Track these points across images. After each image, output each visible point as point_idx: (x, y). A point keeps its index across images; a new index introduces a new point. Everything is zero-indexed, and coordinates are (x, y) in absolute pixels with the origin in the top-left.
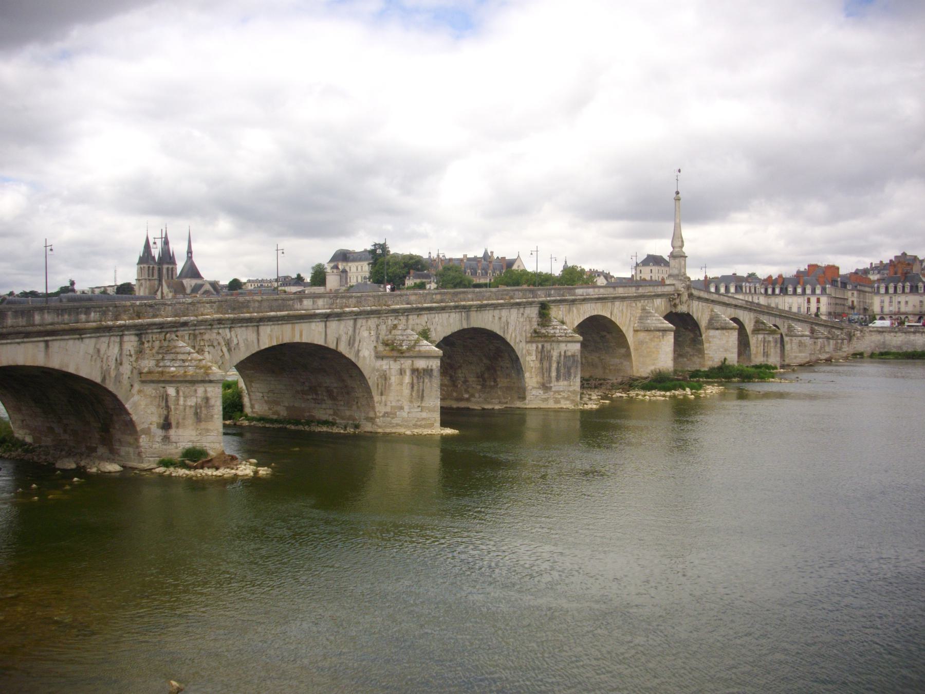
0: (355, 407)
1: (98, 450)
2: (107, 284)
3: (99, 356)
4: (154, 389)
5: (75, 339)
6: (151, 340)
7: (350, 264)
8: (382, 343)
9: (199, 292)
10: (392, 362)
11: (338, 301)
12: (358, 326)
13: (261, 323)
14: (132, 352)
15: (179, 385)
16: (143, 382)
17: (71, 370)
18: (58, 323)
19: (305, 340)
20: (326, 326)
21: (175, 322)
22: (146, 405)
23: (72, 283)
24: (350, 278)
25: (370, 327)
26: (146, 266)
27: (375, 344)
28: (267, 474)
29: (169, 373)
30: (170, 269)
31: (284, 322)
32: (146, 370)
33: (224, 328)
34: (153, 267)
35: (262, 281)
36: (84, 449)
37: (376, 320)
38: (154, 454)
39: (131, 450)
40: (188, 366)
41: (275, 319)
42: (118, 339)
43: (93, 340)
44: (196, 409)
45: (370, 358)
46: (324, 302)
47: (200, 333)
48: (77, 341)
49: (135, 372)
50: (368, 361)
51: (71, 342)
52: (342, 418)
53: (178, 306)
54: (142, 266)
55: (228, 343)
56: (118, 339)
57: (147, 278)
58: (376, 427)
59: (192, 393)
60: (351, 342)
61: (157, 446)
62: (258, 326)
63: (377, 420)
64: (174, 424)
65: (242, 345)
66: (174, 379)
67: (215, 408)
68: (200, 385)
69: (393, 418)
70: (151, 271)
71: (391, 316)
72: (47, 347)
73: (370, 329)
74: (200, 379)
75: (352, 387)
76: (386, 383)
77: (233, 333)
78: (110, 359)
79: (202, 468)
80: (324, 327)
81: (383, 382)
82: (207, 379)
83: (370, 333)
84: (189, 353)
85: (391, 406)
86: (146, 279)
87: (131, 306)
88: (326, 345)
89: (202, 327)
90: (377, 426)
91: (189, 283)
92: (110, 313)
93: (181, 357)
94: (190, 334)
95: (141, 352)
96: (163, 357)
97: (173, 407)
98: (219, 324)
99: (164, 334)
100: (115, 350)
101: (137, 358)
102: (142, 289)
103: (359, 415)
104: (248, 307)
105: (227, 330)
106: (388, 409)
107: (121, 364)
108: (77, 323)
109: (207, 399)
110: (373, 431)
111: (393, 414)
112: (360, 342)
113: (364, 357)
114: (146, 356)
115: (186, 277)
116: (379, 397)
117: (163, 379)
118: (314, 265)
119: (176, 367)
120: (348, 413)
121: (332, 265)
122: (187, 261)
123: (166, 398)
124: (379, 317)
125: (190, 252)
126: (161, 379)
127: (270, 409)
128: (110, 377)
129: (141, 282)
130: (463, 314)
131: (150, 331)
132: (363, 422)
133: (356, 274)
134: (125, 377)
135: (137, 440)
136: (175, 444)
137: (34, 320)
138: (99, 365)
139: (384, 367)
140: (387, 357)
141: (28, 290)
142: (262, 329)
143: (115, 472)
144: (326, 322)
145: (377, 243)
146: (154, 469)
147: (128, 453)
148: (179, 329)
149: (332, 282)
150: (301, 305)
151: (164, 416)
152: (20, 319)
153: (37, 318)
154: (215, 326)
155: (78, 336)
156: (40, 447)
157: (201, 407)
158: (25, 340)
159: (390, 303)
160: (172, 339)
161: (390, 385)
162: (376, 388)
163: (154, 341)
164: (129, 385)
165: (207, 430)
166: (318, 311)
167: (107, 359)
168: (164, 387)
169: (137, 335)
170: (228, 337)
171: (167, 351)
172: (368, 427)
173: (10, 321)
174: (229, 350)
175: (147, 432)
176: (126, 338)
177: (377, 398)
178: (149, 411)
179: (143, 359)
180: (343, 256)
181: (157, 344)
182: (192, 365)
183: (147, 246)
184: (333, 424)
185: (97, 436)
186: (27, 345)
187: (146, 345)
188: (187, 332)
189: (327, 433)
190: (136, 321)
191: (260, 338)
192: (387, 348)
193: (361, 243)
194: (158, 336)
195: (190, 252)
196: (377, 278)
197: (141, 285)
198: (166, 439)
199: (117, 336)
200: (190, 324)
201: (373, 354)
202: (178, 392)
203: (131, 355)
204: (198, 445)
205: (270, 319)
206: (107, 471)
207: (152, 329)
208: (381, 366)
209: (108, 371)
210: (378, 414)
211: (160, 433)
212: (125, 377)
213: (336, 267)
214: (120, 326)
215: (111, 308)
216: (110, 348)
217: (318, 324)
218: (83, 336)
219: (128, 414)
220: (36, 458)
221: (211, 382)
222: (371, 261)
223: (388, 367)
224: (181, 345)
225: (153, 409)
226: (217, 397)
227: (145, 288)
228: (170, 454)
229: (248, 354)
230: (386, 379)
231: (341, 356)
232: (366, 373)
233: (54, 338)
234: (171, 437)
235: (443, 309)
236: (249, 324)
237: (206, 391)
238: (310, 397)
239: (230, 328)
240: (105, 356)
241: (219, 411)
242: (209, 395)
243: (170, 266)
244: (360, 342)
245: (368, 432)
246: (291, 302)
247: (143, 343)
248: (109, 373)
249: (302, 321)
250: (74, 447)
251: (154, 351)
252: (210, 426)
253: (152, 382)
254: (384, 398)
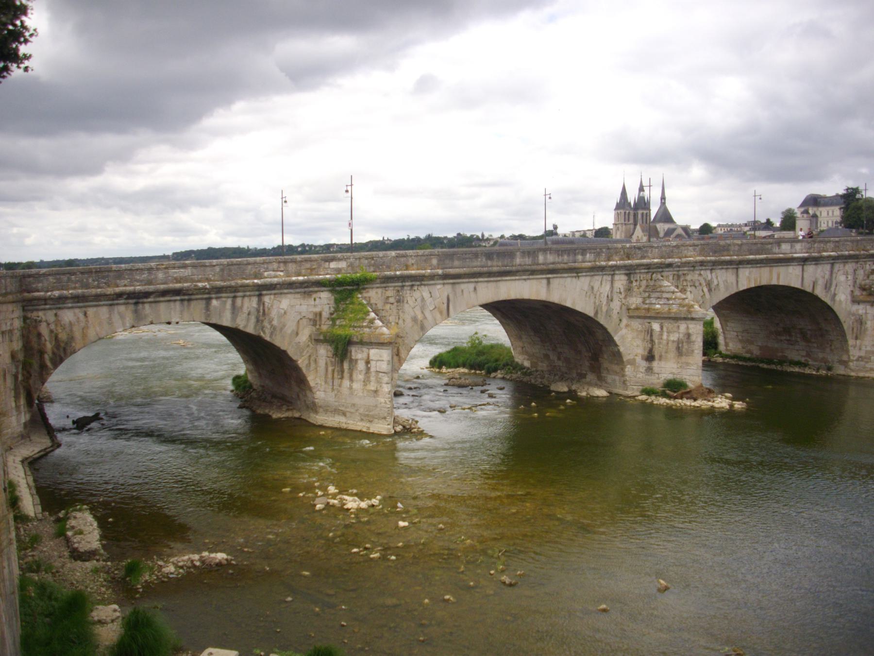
0: (828, 350)
1: (587, 376)
2: (586, 228)
3: (592, 293)
4: (640, 324)
5: (572, 277)
6: (638, 279)
7: (821, 209)
8: (859, 288)
9: (672, 236)
10: (868, 307)
11: (816, 245)
12: (835, 270)
13: (740, 266)
14: (622, 290)
15: (663, 321)
16: (630, 317)
17: (569, 304)
18: (559, 263)
19: (781, 283)
20: (803, 270)
21: (661, 264)
22: (633, 338)
23: (555, 227)
24: (821, 222)
25: (847, 272)
26: (622, 211)
27: (852, 288)
28: (742, 408)
29: (654, 309)
30: (645, 214)
31: (762, 265)
32: (633, 306)
33: (706, 270)
34: (629, 213)
35: (732, 225)
36: (575, 375)
37: (854, 264)
38: (637, 383)
39: (617, 378)
40: (673, 304)
41: (752, 262)
42: (609, 278)
43: (588, 278)
44: (678, 344)
45: (846, 302)
46: (802, 246)
47: (684, 274)
48: (574, 279)
49: (624, 308)
50: (844, 305)
51: (569, 280)
52: (815, 360)
53: (664, 249)
54: (619, 212)
55: (709, 284)
56: (609, 278)
57: (623, 222)
58: (849, 370)
59: (675, 329)
60: (827, 286)
61: (640, 375)
62: (737, 269)
63: (851, 364)
64: (657, 357)
65: (722, 286)
66: (659, 315)
67: (696, 344)
68: (683, 322)
69: (867, 362)
70: (627, 216)
71: (869, 261)
72: (549, 283)
73: (846, 274)
74: (683, 316)
75: (826, 330)
76: (861, 328)
77: (714, 274)
78: (602, 296)
79: (682, 398)
80: (801, 269)
81: (859, 326)
82: (689, 316)
83: (847, 278)
84: (673, 292)
85: (867, 352)
86: (622, 224)
87: (622, 248)
88: (802, 288)
89: (685, 269)
90: (850, 369)
91: (662, 227)
92: (604, 255)
93: (665, 295)
94: (674, 275)
95: (629, 290)
96: (649, 295)
97: (656, 341)
98: (701, 265)
99: (650, 274)
100: (606, 288)
101: (626, 296)
102: (618, 233)
103: (832, 358)
104: (728, 250)
105: (708, 272)
106: (862, 354)
107: (612, 300)
108: (575, 262)
109: (688, 335)
110: (846, 374)
111: (865, 358)
112: (836, 286)
113: (840, 301)
114: (634, 294)
115: (660, 221)
116: (854, 341)
117: (649, 315)
118: (784, 210)
119: (661, 304)
120: (821, 355)
121: (802, 209)
122: (660, 208)
123: (651, 332)
124: (857, 262)
125: (663, 198)
126: (647, 315)
127: (743, 348)
128: (602, 311)
129: (617, 226)
131: (638, 271)
132: (836, 365)
133: (828, 219)
134: (615, 312)
135: (623, 369)
136: (657, 375)
137: (538, 259)
138: (592, 301)
139: (860, 312)
140: (864, 302)
141: (517, 234)
142: (741, 271)
143: (603, 397)
144: (803, 265)
145: (850, 187)
146: (637, 396)
147: (614, 380)
148: (664, 270)
149: (802, 228)
150: (779, 249)
151: (648, 349)
152: (527, 259)
153: (541, 258)
154: (697, 268)
155: (575, 275)
156: (537, 371)
157: (683, 343)
158: (531, 277)
159: (868, 248)
160: (658, 279)
161: (866, 330)
162: (851, 332)
163: (641, 280)
164: (618, 320)
165: (688, 364)
166: (796, 255)
167: (600, 295)
168: (649, 323)
169: (626, 274)
170: (709, 278)
171: (653, 289)
172: (840, 370)
173: (518, 260)
174: (710, 290)
175: (632, 362)
176: (617, 277)
177: (851, 342)
178: (635, 344)
179: (632, 296)
180: (814, 201)
181: (644, 283)
182: (675, 303)
183: (624, 193)
184: (805, 365)
185: (587, 364)
186: (532, 281)
187: (634, 284)
188: (671, 273)
189: (799, 373)
190: (626, 262)
191: (739, 280)
192: (864, 293)
193: (833, 188)
194: (645, 276)
195: (663, 198)
196: (848, 222)
197: (618, 229)
198: (649, 370)
199: (609, 275)
200: (675, 265)
201: (849, 298)
202: (662, 328)
203: (620, 293)
204: (678, 377)
205: (749, 262)
206: (595, 395)
207: (640, 269)
208: (857, 310)
209: (600, 306)
210: (852, 358)
211: (644, 364)
212: (615, 312)
213: (806, 212)
214: (612, 267)
215: (604, 250)
216: (603, 286)
217: (795, 267)
218: (580, 274)
219: (616, 345)
220: (533, 381)
221: (693, 319)
222: (843, 206)
223: (864, 311)
224: (666, 285)
225: (639, 342)
226: (698, 334)
227: (622, 231)
228: (652, 384)
229: (727, 295)
230: (861, 323)
231: (817, 299)
232: (842, 317)
233: (555, 275)
234: (654, 368)
236: (729, 266)
237: (688, 328)
238: (783, 338)
239: (711, 270)
240: (598, 293)
241: (699, 346)
242: (690, 331)
243: (645, 212)
244: (836, 286)
245: (840, 375)
246: (769, 246)
247: (631, 282)
248: (601, 308)
249: (780, 264)
250: (566, 373)
251: (641, 289)
252: (690, 360)
253: (639, 317)
254: (858, 342)
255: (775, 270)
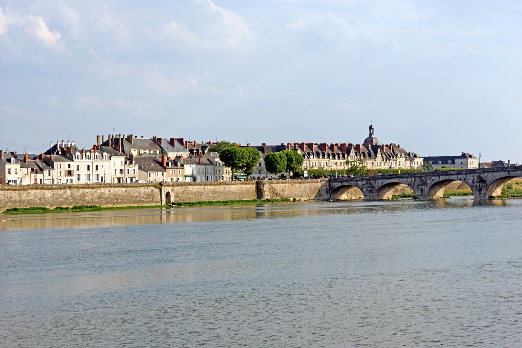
55: (433, 180)
65: (436, 180)
100: (411, 180)
130: (507, 172)
153: (398, 176)
174: (433, 180)
201: (472, 182)
205: (442, 175)
235: (497, 171)
255: (449, 177)
